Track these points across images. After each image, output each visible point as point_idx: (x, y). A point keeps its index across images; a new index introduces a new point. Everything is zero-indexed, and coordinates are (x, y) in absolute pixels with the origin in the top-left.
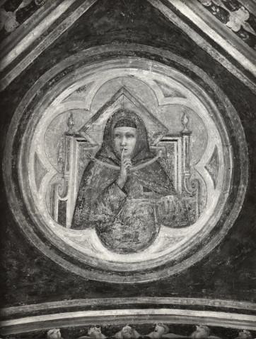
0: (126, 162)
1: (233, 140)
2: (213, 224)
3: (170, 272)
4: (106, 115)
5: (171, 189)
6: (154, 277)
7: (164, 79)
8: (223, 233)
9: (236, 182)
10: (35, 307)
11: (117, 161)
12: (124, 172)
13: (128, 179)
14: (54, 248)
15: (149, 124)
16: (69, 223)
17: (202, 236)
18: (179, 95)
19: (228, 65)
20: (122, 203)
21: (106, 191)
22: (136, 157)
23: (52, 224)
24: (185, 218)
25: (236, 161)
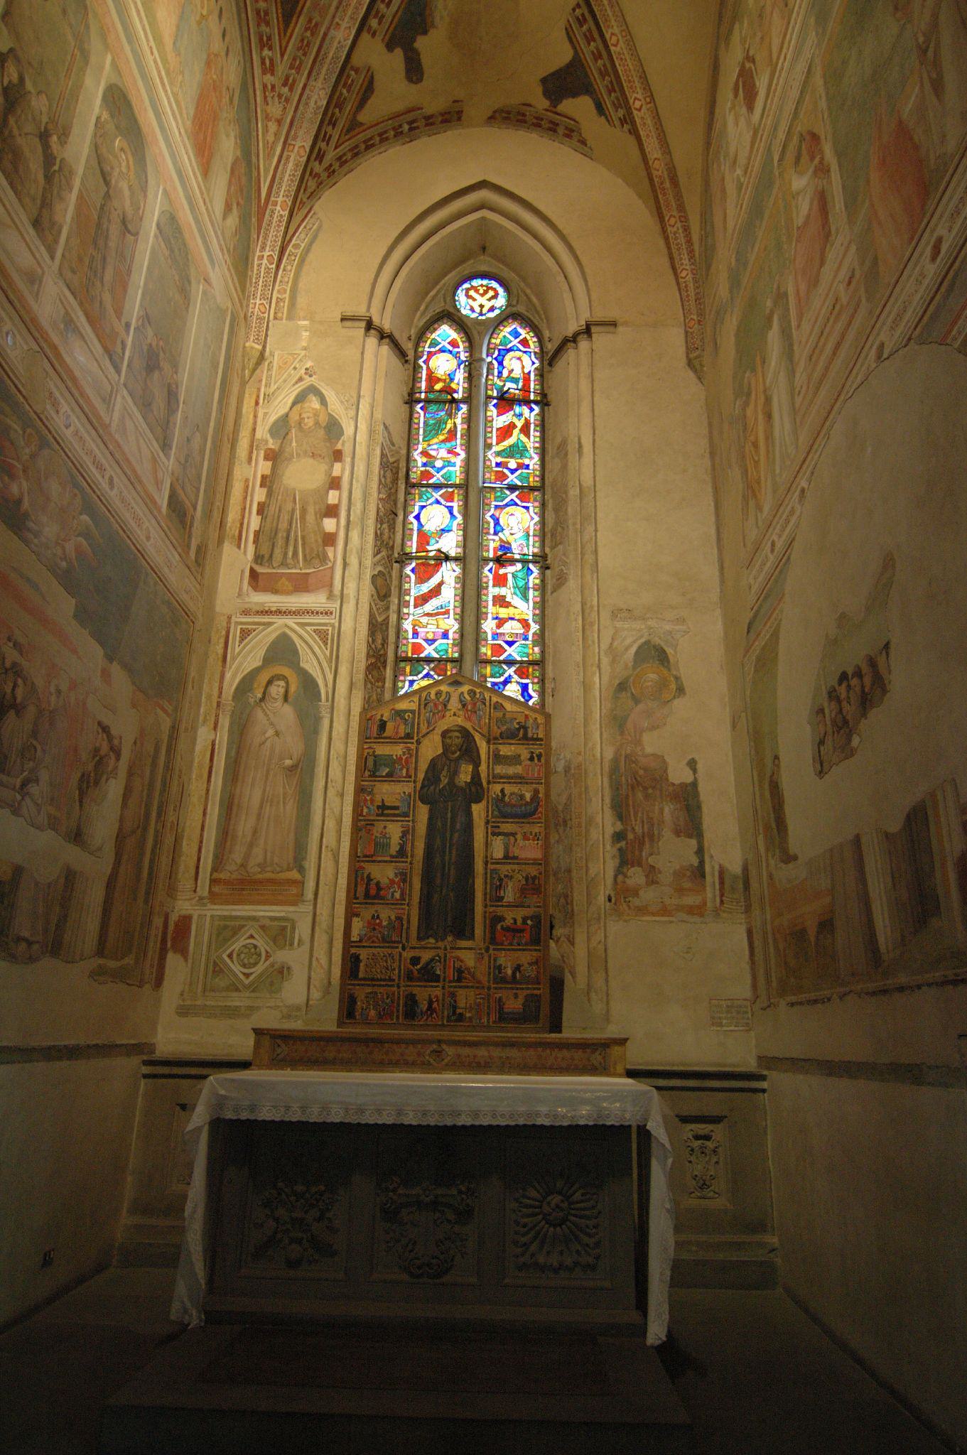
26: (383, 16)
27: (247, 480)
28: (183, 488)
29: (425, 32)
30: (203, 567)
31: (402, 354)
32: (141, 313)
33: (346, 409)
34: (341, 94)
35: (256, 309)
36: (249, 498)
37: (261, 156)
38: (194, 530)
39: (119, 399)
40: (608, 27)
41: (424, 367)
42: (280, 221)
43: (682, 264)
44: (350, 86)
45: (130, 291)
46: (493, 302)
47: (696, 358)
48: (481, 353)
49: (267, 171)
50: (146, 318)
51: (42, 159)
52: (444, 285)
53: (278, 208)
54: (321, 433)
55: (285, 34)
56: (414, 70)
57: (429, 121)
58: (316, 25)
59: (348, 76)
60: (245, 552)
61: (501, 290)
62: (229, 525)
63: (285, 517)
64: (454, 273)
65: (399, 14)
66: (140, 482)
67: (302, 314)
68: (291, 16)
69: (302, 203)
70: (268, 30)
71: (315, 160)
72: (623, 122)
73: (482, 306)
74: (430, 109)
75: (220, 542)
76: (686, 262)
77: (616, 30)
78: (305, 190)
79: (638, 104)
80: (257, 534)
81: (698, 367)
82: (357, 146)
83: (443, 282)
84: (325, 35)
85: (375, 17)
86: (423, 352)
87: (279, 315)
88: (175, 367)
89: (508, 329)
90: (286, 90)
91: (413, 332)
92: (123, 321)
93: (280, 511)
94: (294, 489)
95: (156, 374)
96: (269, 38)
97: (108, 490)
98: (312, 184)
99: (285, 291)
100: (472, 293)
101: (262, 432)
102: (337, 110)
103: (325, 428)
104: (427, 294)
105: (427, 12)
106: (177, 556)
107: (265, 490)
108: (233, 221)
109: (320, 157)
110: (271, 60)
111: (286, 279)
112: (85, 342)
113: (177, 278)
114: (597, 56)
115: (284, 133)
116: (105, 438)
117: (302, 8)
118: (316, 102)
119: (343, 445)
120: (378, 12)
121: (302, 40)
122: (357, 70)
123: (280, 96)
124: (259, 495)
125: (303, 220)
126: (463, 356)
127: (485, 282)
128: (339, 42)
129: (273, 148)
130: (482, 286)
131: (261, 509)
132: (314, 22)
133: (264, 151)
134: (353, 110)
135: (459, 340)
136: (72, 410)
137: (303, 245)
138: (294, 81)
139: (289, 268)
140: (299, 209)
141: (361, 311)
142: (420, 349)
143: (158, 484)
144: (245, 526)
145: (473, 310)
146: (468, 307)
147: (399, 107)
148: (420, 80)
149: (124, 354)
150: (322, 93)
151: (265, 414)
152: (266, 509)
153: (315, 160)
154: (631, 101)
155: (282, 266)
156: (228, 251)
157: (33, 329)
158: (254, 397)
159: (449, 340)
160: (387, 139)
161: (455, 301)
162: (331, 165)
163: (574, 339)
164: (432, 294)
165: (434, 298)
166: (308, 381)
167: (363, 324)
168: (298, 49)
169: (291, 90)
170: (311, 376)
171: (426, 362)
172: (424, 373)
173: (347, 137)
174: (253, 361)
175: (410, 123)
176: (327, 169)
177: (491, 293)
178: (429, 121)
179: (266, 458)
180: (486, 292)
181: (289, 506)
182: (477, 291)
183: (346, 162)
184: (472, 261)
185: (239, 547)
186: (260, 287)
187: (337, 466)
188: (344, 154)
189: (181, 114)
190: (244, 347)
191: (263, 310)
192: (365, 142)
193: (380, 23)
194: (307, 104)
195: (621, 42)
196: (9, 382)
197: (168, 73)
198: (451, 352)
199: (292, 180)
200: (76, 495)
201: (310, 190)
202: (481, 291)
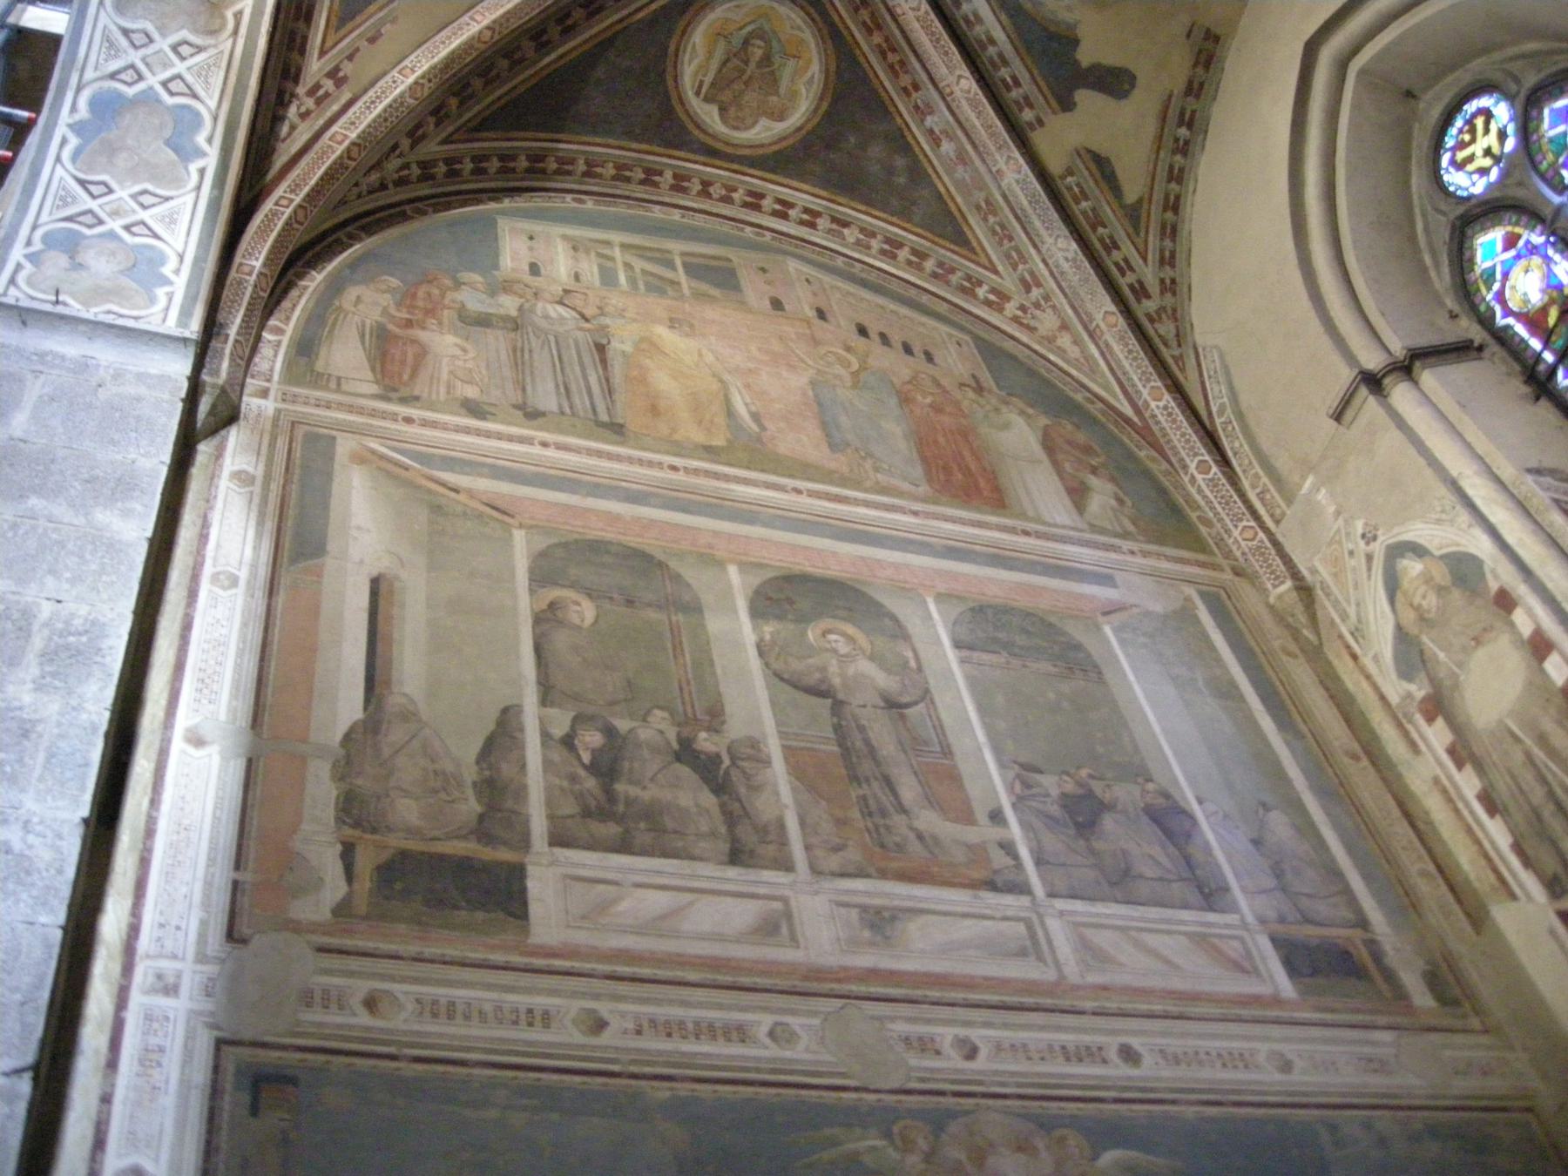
0: (753, 65)
1: (827, 71)
2: (798, 124)
3: (761, 152)
4: (749, 28)
5: (777, 93)
6: (747, 152)
7: (793, 16)
8: (804, 132)
9: (821, 99)
10: (661, 150)
11: (746, 62)
12: (749, 72)
13: (750, 77)
14: (687, 112)
15: (775, 43)
16: (702, 96)
17: (789, 131)
18: (799, 28)
19: (836, 18)
20: (742, 92)
21: (733, 81)
22: (760, 65)
23: (690, 94)
24: (781, 117)
25: (826, 85)
26: (1026, 98)
27: (1436, 781)
28: (1308, 920)
29: (1075, 42)
30: (1471, 996)
31: (1462, 350)
32: (1011, 774)
33: (1452, 522)
34: (1084, 213)
35: (1243, 544)
36: (1460, 805)
37: (1086, 381)
38: (1392, 958)
39: (1054, 925)
41: (1510, 321)
42: (1170, 414)
44: (1082, 191)
45: (965, 768)
46: (1494, 127)
48: (1548, 201)
49: (1107, 388)
50: (1025, 773)
51: (695, 777)
52: (1420, 197)
53: (1153, 404)
54: (1456, 595)
55: (975, 253)
56: (1114, 82)
57: (1194, 89)
58: (988, 202)
59: (1070, 189)
60: (1529, 898)
61: (1485, 102)
62: (1472, 877)
63: (1528, 778)
64: (1414, 169)
65: (1036, 72)
66: (1195, 997)
67: (1296, 478)
68: (962, 233)
69: (1179, 359)
70: (959, 274)
71: (1139, 301)
73: (1488, 152)
74: (1179, 85)
75: (1478, 918)
78: (1166, 344)
80: (1518, 848)
82: (1163, 227)
83: (1415, 197)
84: (1005, 197)
85: (1021, 110)
86: (1488, 304)
87: (1278, 512)
88: (1141, 774)
89: (1546, 124)
90: (1036, 293)
91: (1450, 303)
92: (981, 815)
93: (1513, 777)
94: (1500, 722)
95: (1108, 822)
96: (969, 278)
97: (1135, 1072)
98: (1166, 328)
99: (1256, 476)
100: (1461, 155)
101: (1395, 688)
102: (1101, 230)
103: (1454, 584)
104: (1413, 238)
105: (1052, 29)
106: (1387, 1036)
107: (1468, 768)
108: (1102, 495)
109: (1141, 291)
110: (993, 291)
111: (1246, 462)
112: (922, 911)
113: (1045, 666)
115: (1080, 328)
116: (1066, 1003)
117: (960, 210)
118: (1067, 259)
119: (1496, 577)
120: (1017, 103)
121: (994, 233)
122: (1070, 172)
123: (1037, 305)
124: (1468, 784)
125: (1201, 375)
126: (1537, 239)
127: (1459, 123)
128: (1017, 182)
129: (1088, 358)
130: (1461, 131)
131: (1491, 804)
132: (983, 205)
133: (1079, 370)
134: (1115, 206)
135: (1509, 228)
136: (967, 1024)
137: (1225, 400)
138: (1032, 273)
139: (1237, 444)
140: (1182, 370)
141: (1347, 375)
142: (1482, 308)
143: (1244, 966)
144: (1492, 853)
145: (1483, 172)
146: (1475, 177)
147: (1150, 127)
148: (1132, 79)
149: (1016, 857)
150: (1062, 243)
151: (1376, 658)
152: (1494, 795)
153: (1139, 301)
155: (1230, 454)
156: (1125, 535)
157: (813, 986)
158: (1344, 652)
159: (1499, 246)
160: (1181, 170)
161: (1453, 195)
162: (1162, 281)
164: (1420, 226)
165: (1426, 229)
166: (1378, 549)
167: (1363, 391)
168: (1000, 244)
169: (1039, 285)
170: (1375, 538)
171: (1508, 312)
172: (1520, 330)
173: (1142, 234)
174: (1299, 610)
175: (1181, 123)
176: (1163, 290)
177: (1480, 122)
178: (1194, 89)
179: (1430, 720)
180: (1473, 131)
181: (1519, 757)
182: (1462, 145)
183: (1173, 255)
184: (1417, 125)
185: (1513, 896)
186: (1223, 515)
187: (1519, 616)
188: (1162, 251)
189: (900, 494)
190: (1271, 608)
191: (1249, 534)
192: (1165, 209)
193: (1031, 106)
194: (1062, 273)
196: (814, 1093)
197: (843, 482)
198: (1518, 257)
199: (1135, 359)
200: (1062, 1140)
201: (1171, 336)
202: (1467, 137)
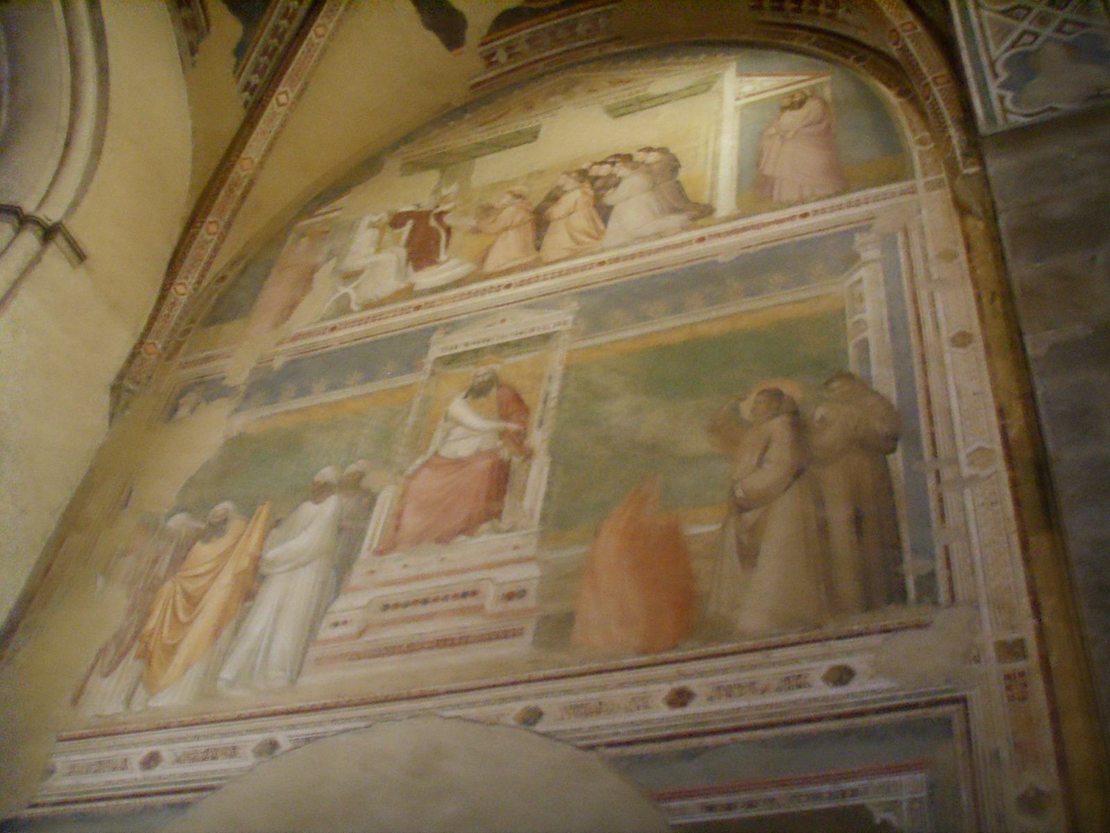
40: (328, 17)
43: (186, 278)
47: (129, 391)
72: (248, 87)
76: (193, 279)
77: (331, 26)
79: (283, 98)
81: (122, 403)
114: (288, 15)
154: (281, 89)
163: (22, 220)
195: (323, 40)
